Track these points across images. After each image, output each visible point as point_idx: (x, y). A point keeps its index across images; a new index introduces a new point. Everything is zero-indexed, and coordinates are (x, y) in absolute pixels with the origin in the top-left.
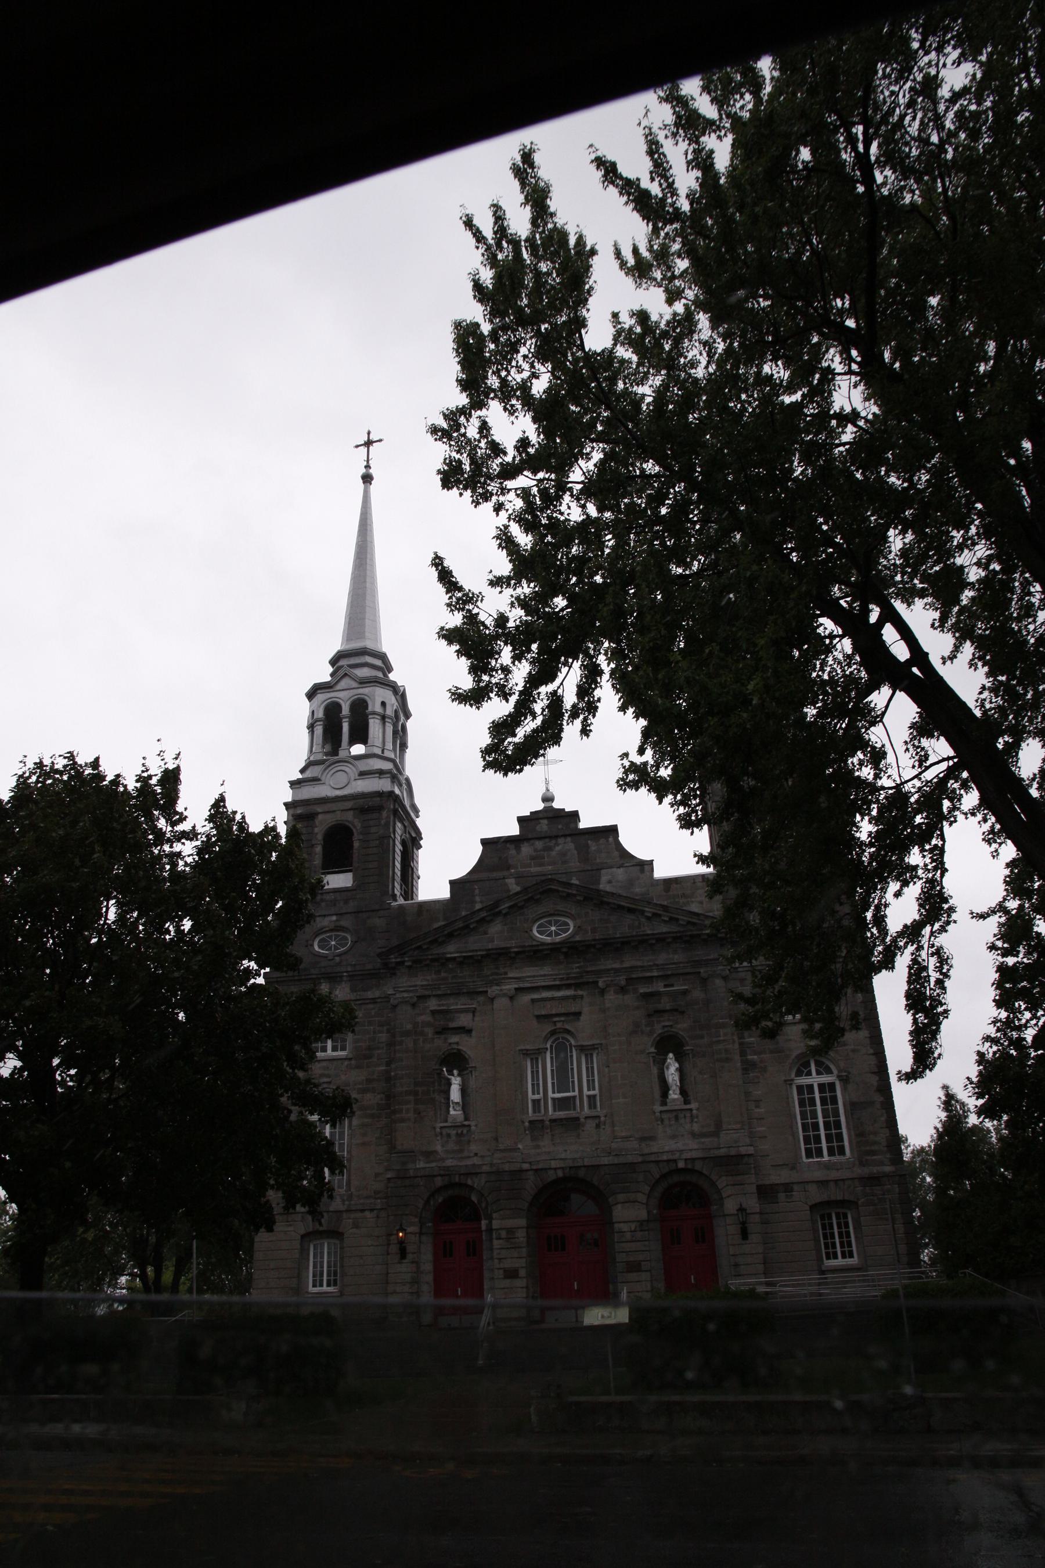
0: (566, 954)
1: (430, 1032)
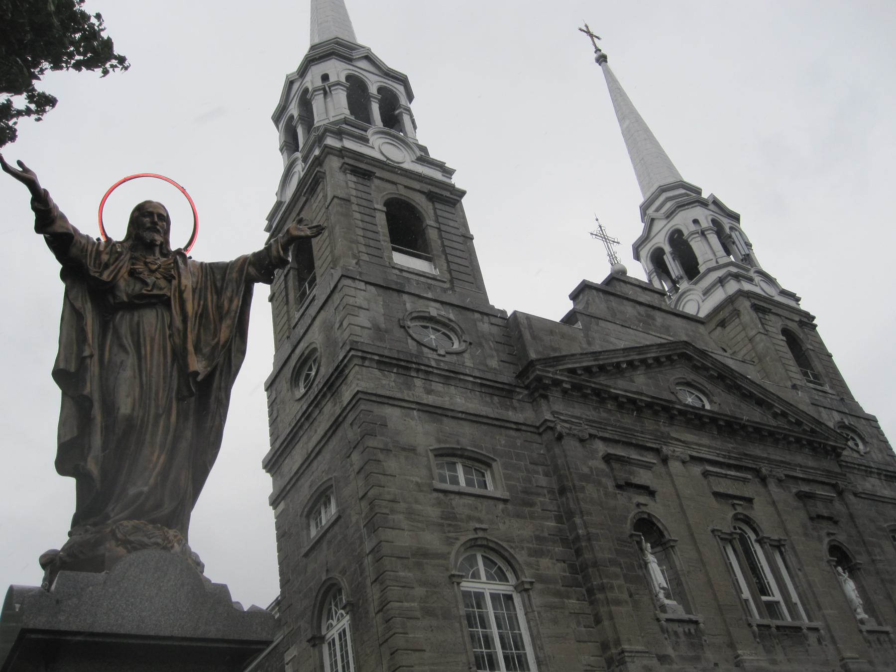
0: (719, 428)
1: (610, 484)
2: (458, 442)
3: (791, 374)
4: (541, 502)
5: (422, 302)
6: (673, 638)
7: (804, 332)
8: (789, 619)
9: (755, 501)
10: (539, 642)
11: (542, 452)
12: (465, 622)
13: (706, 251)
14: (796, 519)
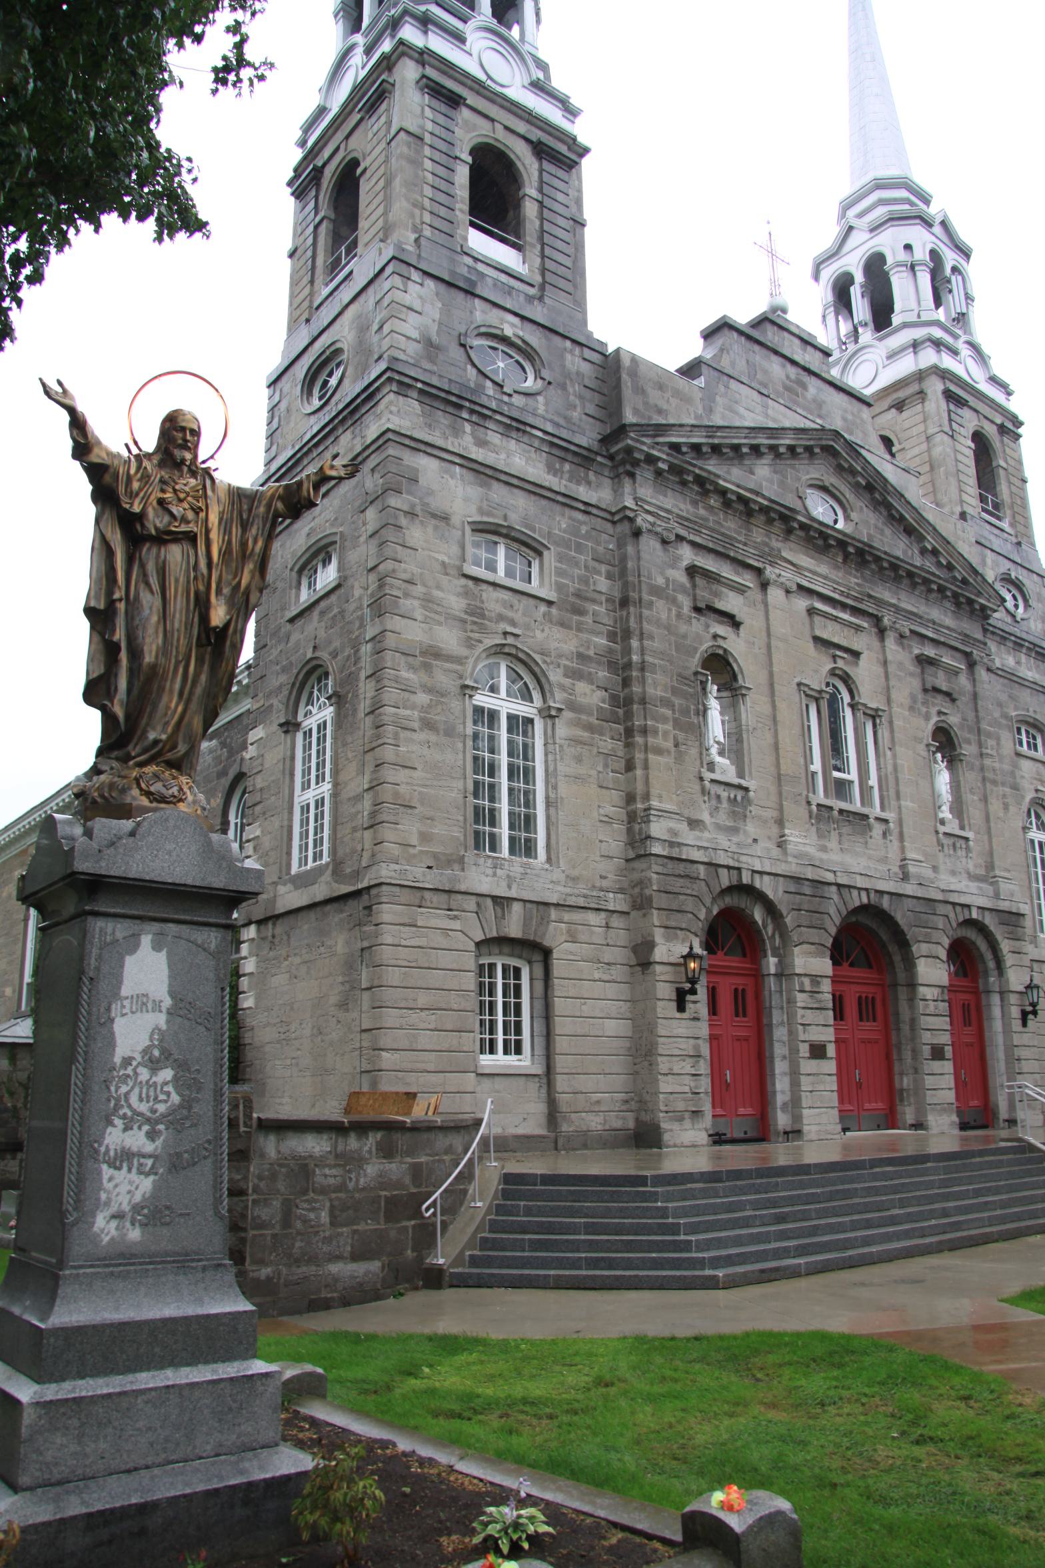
0: (846, 556)
1: (686, 603)
2: (505, 518)
3: (965, 497)
4: (594, 611)
5: (496, 312)
6: (714, 802)
7: (1002, 442)
8: (858, 804)
9: (862, 656)
10: (553, 780)
11: (611, 547)
12: (470, 743)
13: (910, 295)
14: (906, 687)
